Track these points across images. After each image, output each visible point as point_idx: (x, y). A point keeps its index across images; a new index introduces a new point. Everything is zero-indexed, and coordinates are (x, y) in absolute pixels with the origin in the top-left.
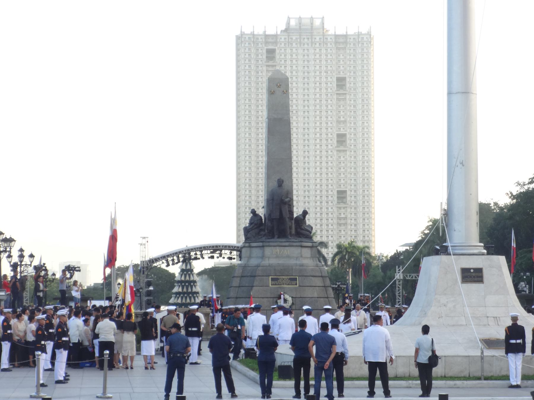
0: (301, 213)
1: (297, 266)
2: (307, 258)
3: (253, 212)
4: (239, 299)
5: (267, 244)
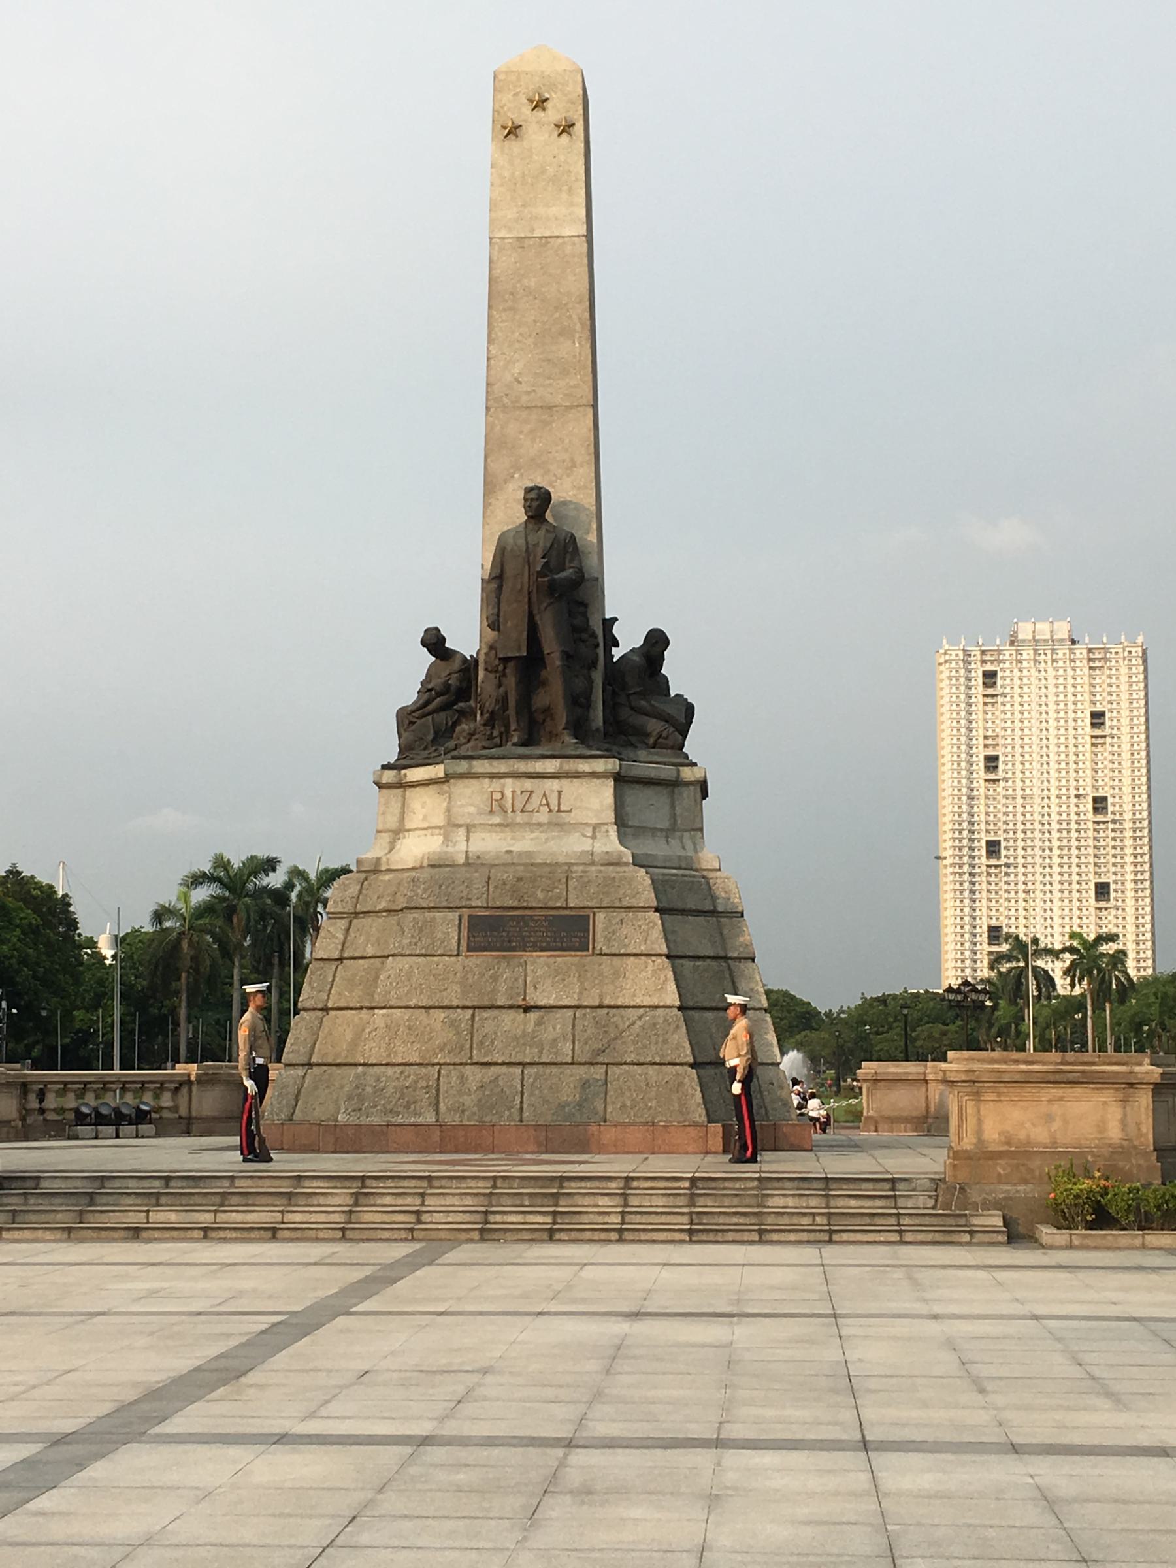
0: (639, 643)
1: (593, 863)
2: (654, 830)
3: (434, 642)
4: (332, 1013)
5: (463, 766)
